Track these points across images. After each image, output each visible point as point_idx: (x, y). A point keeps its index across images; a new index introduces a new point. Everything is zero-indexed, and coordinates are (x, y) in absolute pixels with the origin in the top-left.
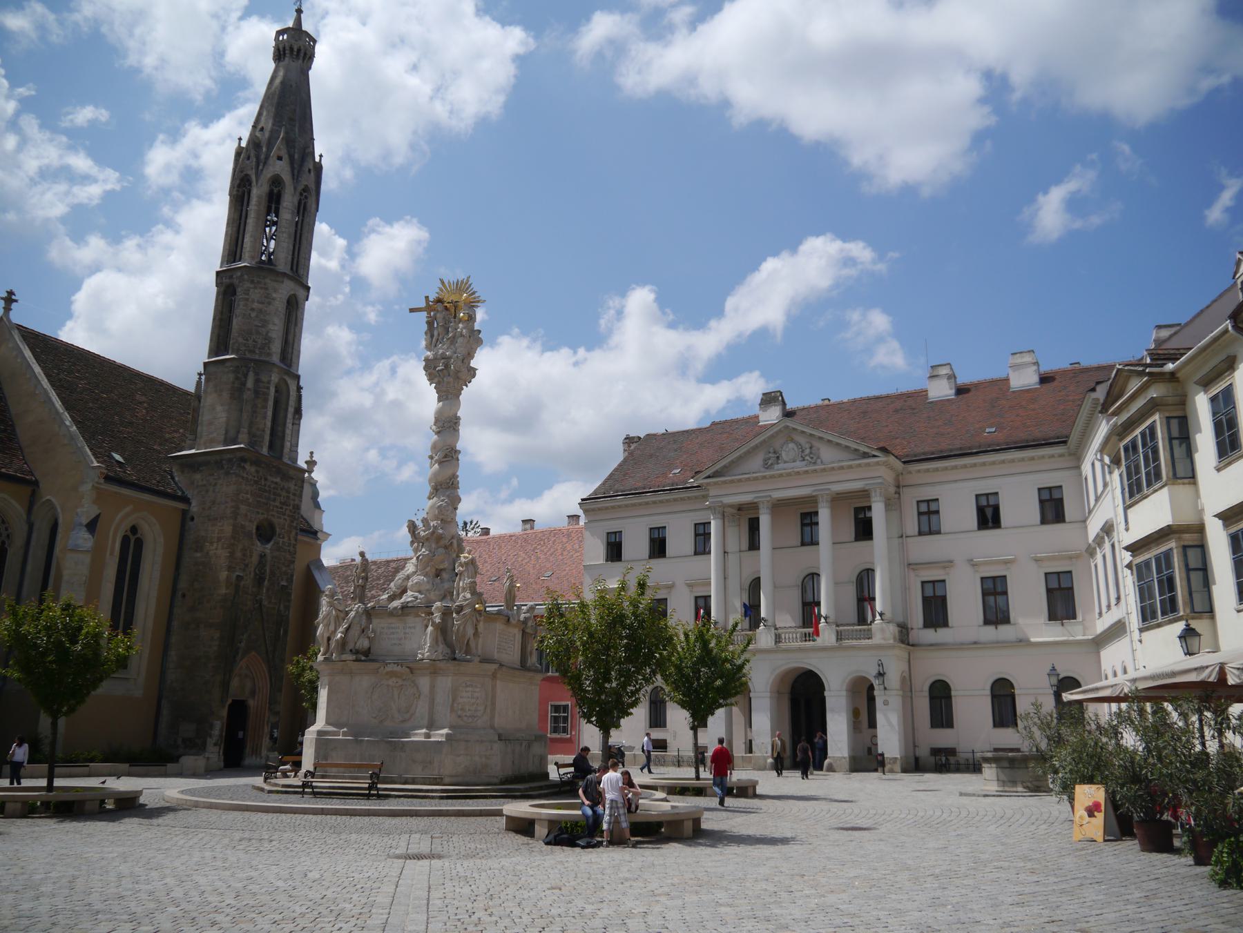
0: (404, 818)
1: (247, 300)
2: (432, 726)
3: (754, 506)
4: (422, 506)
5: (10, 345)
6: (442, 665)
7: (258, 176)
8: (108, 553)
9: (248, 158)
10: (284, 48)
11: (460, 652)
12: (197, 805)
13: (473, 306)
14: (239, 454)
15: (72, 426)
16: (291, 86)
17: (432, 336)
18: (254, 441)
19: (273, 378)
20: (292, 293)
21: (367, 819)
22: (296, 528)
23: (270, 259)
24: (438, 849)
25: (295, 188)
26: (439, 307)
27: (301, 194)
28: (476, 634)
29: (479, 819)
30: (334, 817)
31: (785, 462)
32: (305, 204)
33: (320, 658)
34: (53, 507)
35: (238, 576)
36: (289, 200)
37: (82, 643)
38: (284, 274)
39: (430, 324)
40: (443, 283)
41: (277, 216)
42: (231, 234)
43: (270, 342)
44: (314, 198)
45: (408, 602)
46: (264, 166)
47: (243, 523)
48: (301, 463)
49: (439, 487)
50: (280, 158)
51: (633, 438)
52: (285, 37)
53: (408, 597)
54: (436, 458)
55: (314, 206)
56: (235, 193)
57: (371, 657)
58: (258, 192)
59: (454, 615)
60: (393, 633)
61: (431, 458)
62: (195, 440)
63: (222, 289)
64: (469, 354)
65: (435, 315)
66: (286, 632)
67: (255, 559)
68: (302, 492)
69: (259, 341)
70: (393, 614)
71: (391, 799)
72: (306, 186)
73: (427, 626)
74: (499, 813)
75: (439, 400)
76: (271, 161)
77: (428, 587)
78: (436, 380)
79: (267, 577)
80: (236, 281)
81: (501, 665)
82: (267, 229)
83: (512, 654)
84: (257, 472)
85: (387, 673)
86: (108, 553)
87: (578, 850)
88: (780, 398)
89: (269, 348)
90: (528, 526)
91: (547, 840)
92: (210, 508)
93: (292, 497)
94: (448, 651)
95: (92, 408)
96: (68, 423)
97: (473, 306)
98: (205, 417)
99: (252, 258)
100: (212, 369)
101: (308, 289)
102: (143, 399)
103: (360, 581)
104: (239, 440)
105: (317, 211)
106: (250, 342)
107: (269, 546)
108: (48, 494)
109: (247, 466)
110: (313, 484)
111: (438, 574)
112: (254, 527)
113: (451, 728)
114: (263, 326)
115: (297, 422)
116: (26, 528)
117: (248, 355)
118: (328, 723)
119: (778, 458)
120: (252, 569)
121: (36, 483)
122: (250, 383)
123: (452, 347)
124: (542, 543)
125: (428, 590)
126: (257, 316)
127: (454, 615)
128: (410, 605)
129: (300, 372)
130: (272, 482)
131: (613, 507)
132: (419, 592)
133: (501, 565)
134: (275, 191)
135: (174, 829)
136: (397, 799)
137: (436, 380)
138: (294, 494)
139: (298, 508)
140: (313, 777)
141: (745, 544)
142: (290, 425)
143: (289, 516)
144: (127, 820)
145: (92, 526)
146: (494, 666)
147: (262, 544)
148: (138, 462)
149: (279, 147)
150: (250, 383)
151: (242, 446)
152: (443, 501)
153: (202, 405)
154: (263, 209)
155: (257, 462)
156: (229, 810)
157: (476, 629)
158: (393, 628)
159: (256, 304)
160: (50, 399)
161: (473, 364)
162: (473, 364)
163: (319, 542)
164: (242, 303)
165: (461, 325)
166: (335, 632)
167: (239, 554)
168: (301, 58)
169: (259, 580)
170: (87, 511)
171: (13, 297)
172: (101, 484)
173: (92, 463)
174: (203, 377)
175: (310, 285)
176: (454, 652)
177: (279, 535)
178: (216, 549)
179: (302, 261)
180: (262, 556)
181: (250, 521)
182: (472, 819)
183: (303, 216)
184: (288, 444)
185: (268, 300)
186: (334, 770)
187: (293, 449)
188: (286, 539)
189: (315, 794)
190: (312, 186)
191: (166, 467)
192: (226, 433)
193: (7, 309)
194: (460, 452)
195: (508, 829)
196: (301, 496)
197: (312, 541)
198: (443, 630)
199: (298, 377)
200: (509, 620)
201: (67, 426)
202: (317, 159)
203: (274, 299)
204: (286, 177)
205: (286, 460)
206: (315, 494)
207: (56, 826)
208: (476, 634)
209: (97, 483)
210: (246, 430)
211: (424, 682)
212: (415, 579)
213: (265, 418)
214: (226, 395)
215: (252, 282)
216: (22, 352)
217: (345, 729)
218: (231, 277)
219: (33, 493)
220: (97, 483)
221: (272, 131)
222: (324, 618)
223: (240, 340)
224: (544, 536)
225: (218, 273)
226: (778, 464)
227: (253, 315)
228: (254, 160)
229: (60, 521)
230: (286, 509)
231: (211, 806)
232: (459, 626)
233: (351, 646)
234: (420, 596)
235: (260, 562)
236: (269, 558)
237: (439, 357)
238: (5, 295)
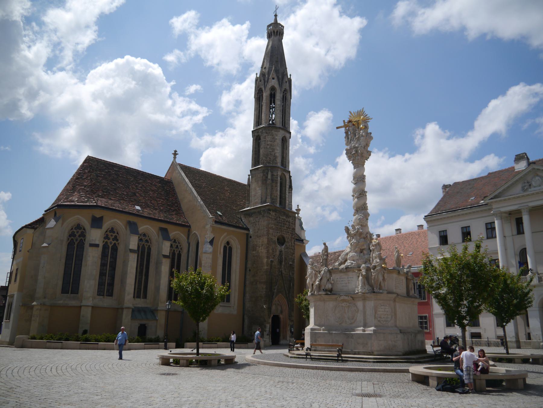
0: (357, 373)
1: (265, 141)
2: (365, 326)
3: (519, 211)
4: (351, 219)
5: (177, 172)
6: (368, 295)
7: (265, 88)
8: (219, 254)
9: (261, 81)
10: (271, 32)
11: (376, 288)
12: (259, 363)
13: (366, 122)
14: (267, 208)
15: (201, 202)
16: (275, 47)
17: (348, 139)
18: (273, 201)
19: (279, 173)
20: (284, 135)
21: (338, 372)
22: (294, 238)
23: (273, 122)
24: (378, 391)
25: (281, 90)
26: (350, 124)
27: (284, 93)
28: (384, 279)
29: (396, 374)
30: (322, 371)
31: (535, 187)
32: (286, 96)
33: (309, 294)
34: (197, 236)
35: (271, 260)
36: (279, 96)
37: (206, 289)
38: (280, 128)
39: (346, 133)
40: (350, 113)
41: (274, 104)
42: (257, 114)
43: (276, 158)
44: (289, 93)
45: (349, 266)
47: (272, 237)
48: (294, 209)
49: (358, 210)
50: (273, 79)
51: (447, 185)
52: (271, 27)
53: (348, 263)
54: (356, 195)
55: (289, 97)
57: (333, 292)
59: (372, 270)
60: (343, 281)
61: (353, 196)
62: (249, 203)
63: (255, 138)
64: (367, 144)
65: (348, 128)
66: (293, 285)
67: (278, 253)
68: (295, 222)
69: (272, 158)
70: (342, 271)
71: (348, 362)
72: (285, 89)
73: (359, 277)
74: (407, 371)
75: (354, 168)
76: (270, 80)
77: (357, 258)
78: (352, 159)
79: (284, 261)
80: (260, 134)
81: (398, 295)
82: (271, 110)
83: (402, 289)
84: (276, 215)
85: (342, 300)
86: (219, 254)
87: (457, 395)
88: (526, 156)
89: (276, 160)
90: (398, 232)
91: (438, 388)
92: (257, 232)
93: (291, 225)
94: (370, 288)
95: (208, 194)
96: (199, 201)
97: (366, 122)
98: (252, 193)
99: (266, 123)
100: (253, 172)
102: (228, 189)
103: (325, 256)
104: (267, 201)
105: (291, 99)
106: (268, 159)
107: (283, 247)
108: (194, 231)
109: (271, 212)
110: (300, 219)
111: (362, 251)
112: (276, 239)
113: (375, 326)
114: (272, 152)
115: (291, 192)
116: (187, 245)
117: (268, 165)
118: (315, 324)
119: (530, 185)
120: (277, 257)
121: (189, 227)
122: (269, 177)
123: (358, 142)
124: (406, 239)
125: (357, 259)
126: (270, 147)
127: (372, 270)
128: (349, 267)
129: (290, 170)
130: (282, 219)
131: (441, 219)
132: (354, 260)
133: (387, 251)
135: (248, 375)
136: (352, 362)
137: (352, 159)
138: (292, 224)
139: (294, 229)
140: (310, 351)
141: (515, 231)
142: (288, 193)
143: (290, 233)
144: (229, 370)
145: (211, 242)
146: (394, 295)
147: (280, 246)
148: (227, 215)
149: (273, 74)
150: (269, 177)
151: (268, 204)
152: (361, 216)
153: (251, 188)
154: (269, 102)
155: (275, 210)
156: (273, 366)
157: (384, 277)
158: (342, 278)
160: (192, 191)
161: (369, 149)
162: (369, 149)
163: (304, 244)
165: (361, 131)
166: (315, 281)
167: (271, 251)
168: (278, 35)
169: (280, 262)
170: (209, 236)
171: (177, 153)
172: (213, 224)
173: (210, 216)
174: (250, 176)
176: (373, 289)
177: (287, 242)
178: (261, 249)
179: (286, 121)
180: (281, 251)
181: (274, 236)
182: (392, 374)
183: (285, 102)
184: (287, 202)
185: (274, 140)
186: (320, 347)
187: (290, 204)
188: (290, 244)
189: (312, 359)
190: (288, 88)
191: (239, 216)
192: (261, 199)
193: (175, 158)
194: (367, 192)
195: (413, 380)
196: (295, 224)
197: (301, 244)
198: (367, 278)
199: (289, 172)
200: (399, 272)
201: (199, 202)
202: (289, 77)
203: (276, 139)
204: (277, 86)
205: (287, 209)
206: (301, 224)
207: (199, 371)
208: (384, 279)
209: (212, 224)
210: (269, 197)
211: (360, 304)
212: (351, 254)
213: (277, 191)
214: (260, 183)
215: (267, 133)
216: (181, 174)
217: (323, 328)
218: (258, 132)
219: (189, 231)
220: (212, 224)
221: (269, 68)
222: (309, 275)
223: (264, 158)
224: (406, 236)
225: (252, 131)
226: (530, 188)
227: (268, 147)
228: (263, 81)
229: (200, 241)
230: (289, 230)
231: (265, 364)
232: (375, 275)
233: (323, 288)
234: (354, 262)
235: (280, 254)
236: (283, 252)
237: (352, 148)
238: (174, 152)
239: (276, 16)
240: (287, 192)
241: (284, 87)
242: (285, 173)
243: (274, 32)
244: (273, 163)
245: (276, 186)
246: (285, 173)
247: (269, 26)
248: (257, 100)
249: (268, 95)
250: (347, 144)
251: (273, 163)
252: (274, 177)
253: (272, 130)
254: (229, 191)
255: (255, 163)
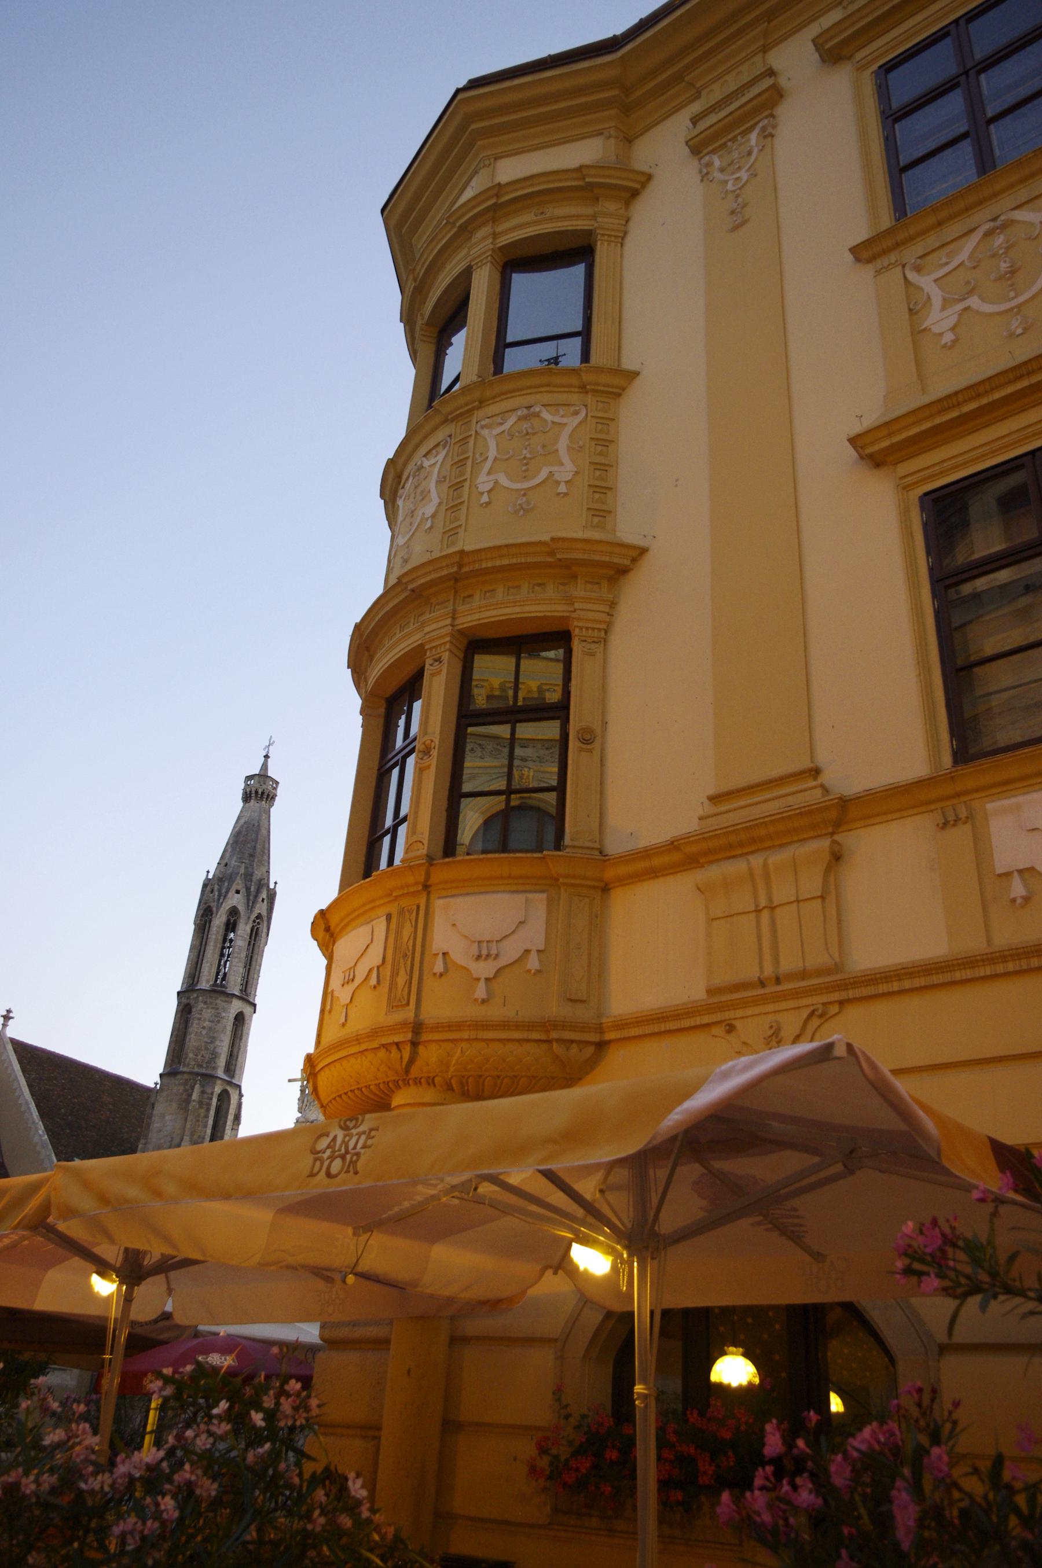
9: (212, 891)
10: (251, 791)
15: (44, 1136)
16: (254, 825)
17: (303, 1102)
19: (216, 1090)
20: (240, 1011)
27: (254, 921)
36: (244, 928)
38: (233, 995)
39: (302, 1091)
42: (192, 959)
43: (215, 1058)
46: (224, 900)
50: (238, 892)
52: (252, 782)
55: (265, 930)
56: (198, 922)
58: (219, 921)
63: (181, 1007)
76: (230, 895)
80: (192, 1002)
101: (254, 1005)
114: (212, 1042)
115: (236, 1128)
117: (196, 1070)
122: (195, 1096)
134: (232, 921)
159: (207, 1023)
164: (196, 1022)
175: (257, 1001)
185: (217, 1018)
190: (264, 913)
199: (239, 1087)
202: (272, 886)
203: (223, 1018)
213: (206, 1126)
214: (175, 1105)
215: (205, 1003)
218: (188, 998)
225: (179, 993)
227: (204, 1032)
228: (217, 893)
239: (267, 757)
240: (227, 1128)
241: (256, 912)
242: (229, 1088)
243: (256, 792)
244: (207, 1067)
245: (207, 1116)
246: (229, 1088)
247: (249, 778)
248: (199, 929)
249: (222, 925)
250: (300, 1110)
251: (207, 1067)
252: (206, 1096)
253: (215, 1000)
254: (111, 1106)
255: (172, 1061)
